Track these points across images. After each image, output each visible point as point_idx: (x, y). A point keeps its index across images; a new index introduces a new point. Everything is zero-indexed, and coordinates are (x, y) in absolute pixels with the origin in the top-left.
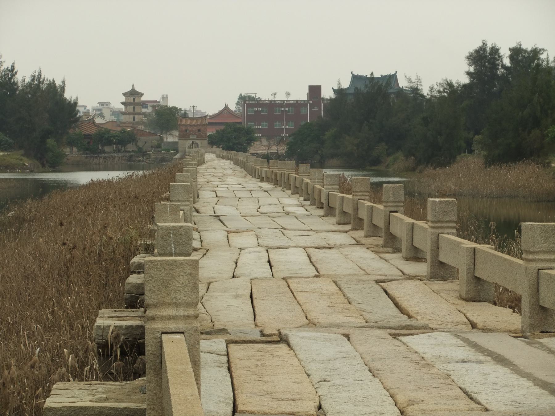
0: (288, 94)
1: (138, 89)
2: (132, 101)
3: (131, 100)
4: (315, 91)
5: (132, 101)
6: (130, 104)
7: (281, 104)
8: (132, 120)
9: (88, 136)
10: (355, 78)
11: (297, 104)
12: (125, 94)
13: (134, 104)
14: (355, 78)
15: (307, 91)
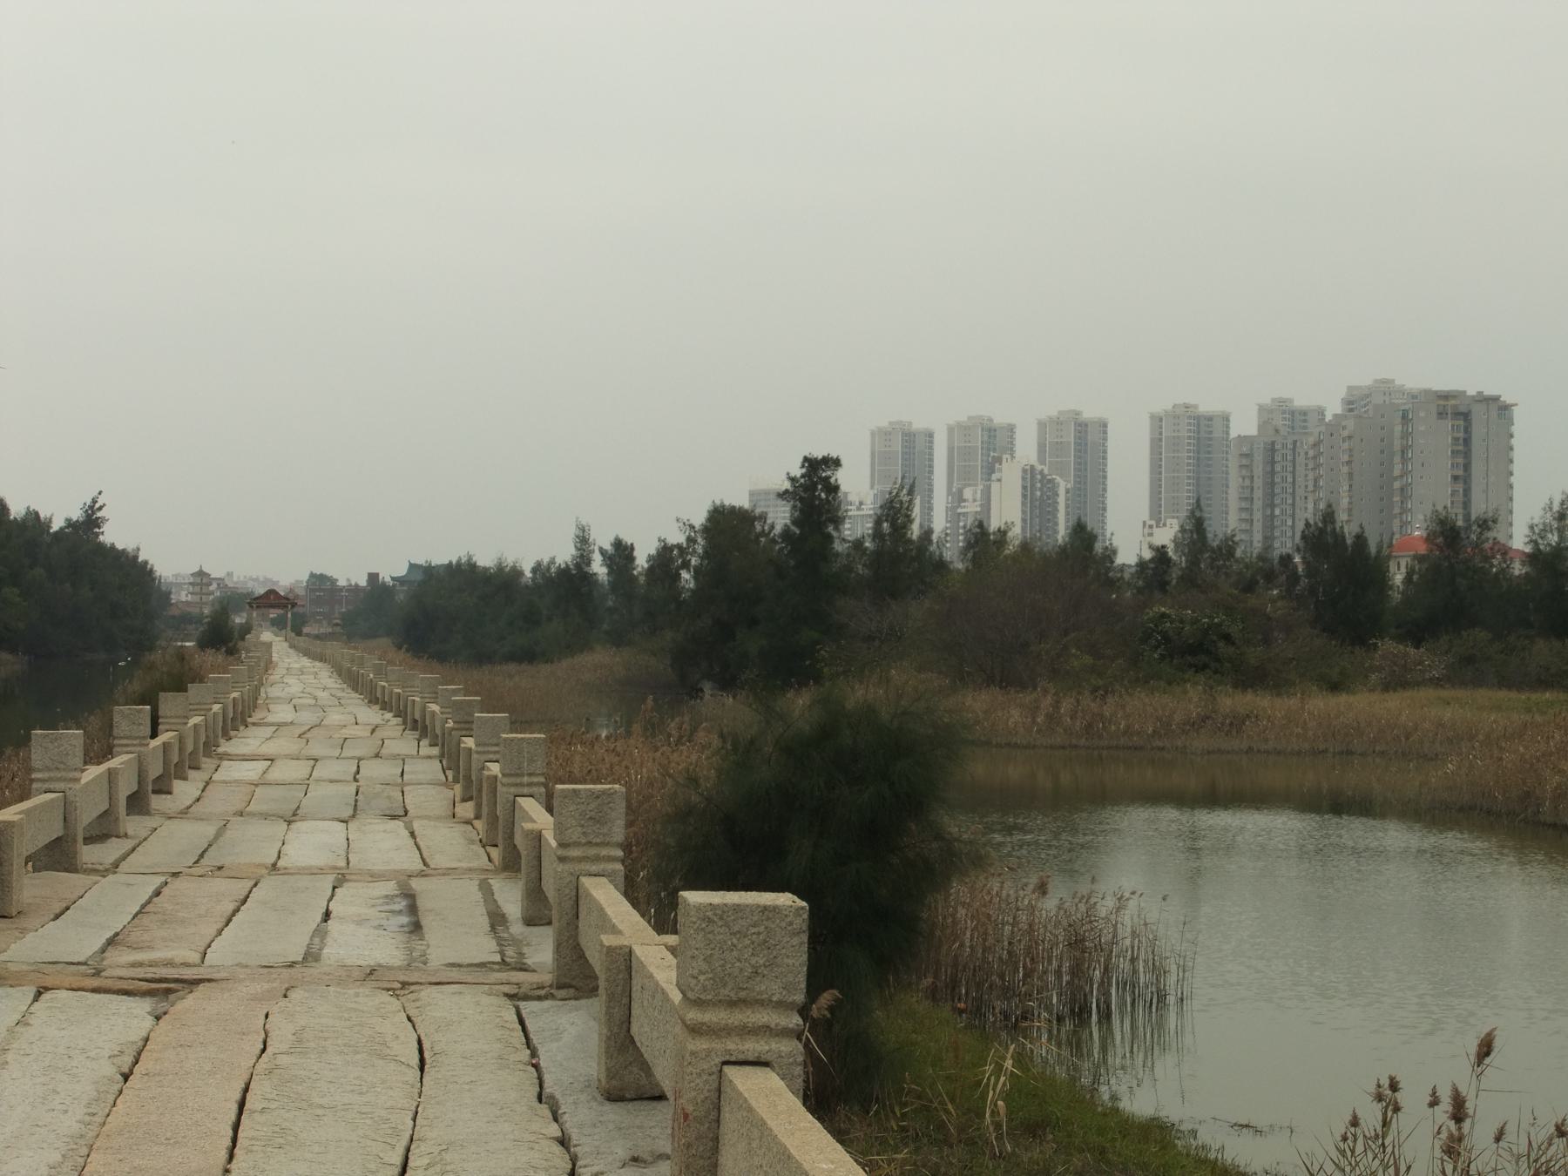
0: (348, 580)
1: (205, 570)
2: (199, 581)
3: (198, 580)
4: (373, 577)
5: (199, 581)
6: (198, 584)
7: (341, 589)
8: (198, 600)
9: (173, 617)
10: (412, 567)
11: (355, 589)
12: (192, 575)
13: (201, 584)
14: (412, 567)
15: (366, 578)
